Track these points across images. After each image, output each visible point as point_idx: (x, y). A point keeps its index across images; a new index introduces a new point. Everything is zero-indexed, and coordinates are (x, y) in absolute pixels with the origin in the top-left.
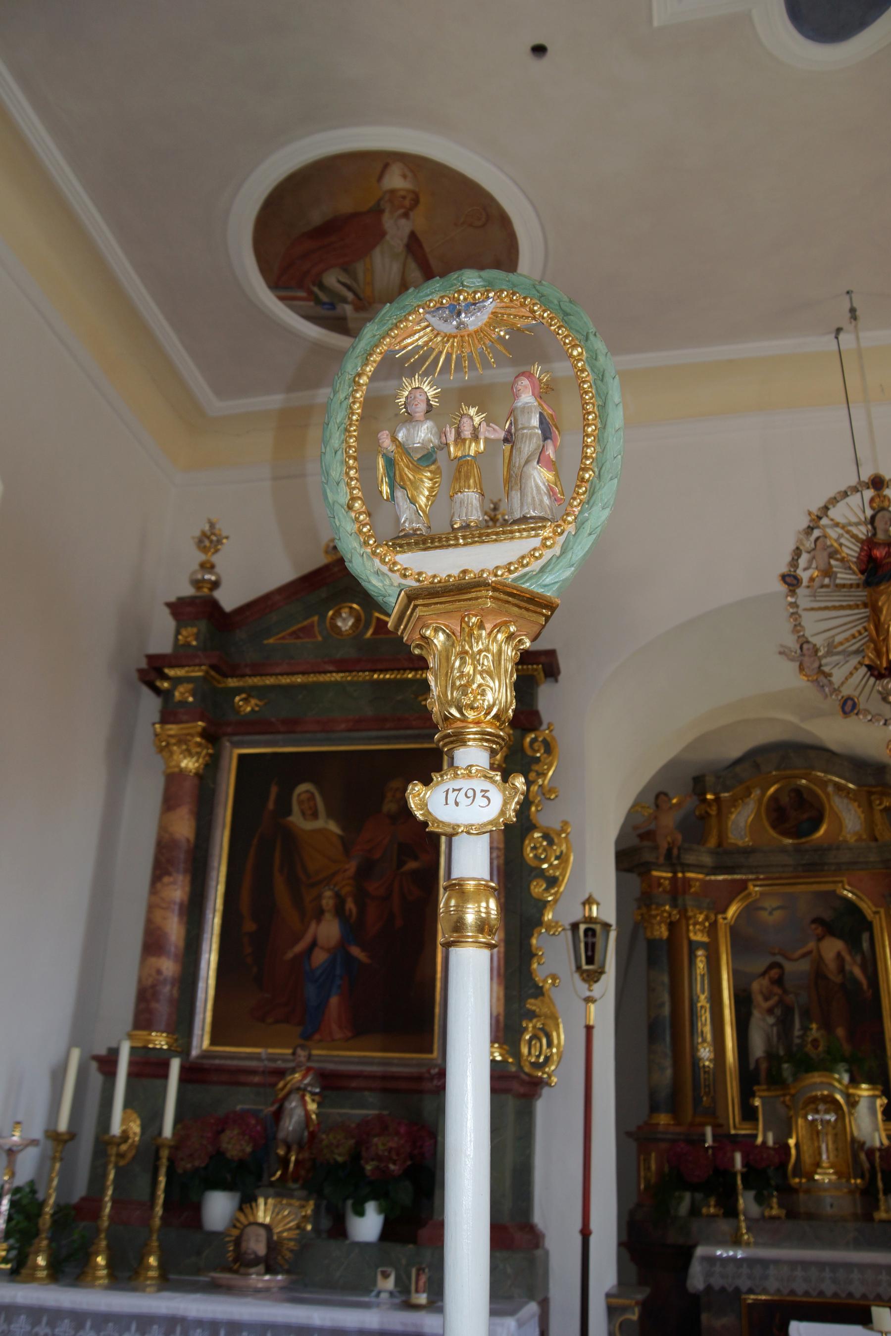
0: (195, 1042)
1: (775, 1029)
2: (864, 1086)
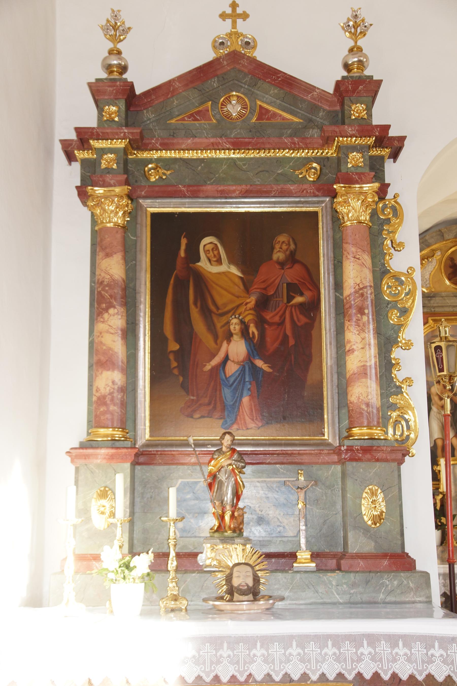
0: (139, 432)
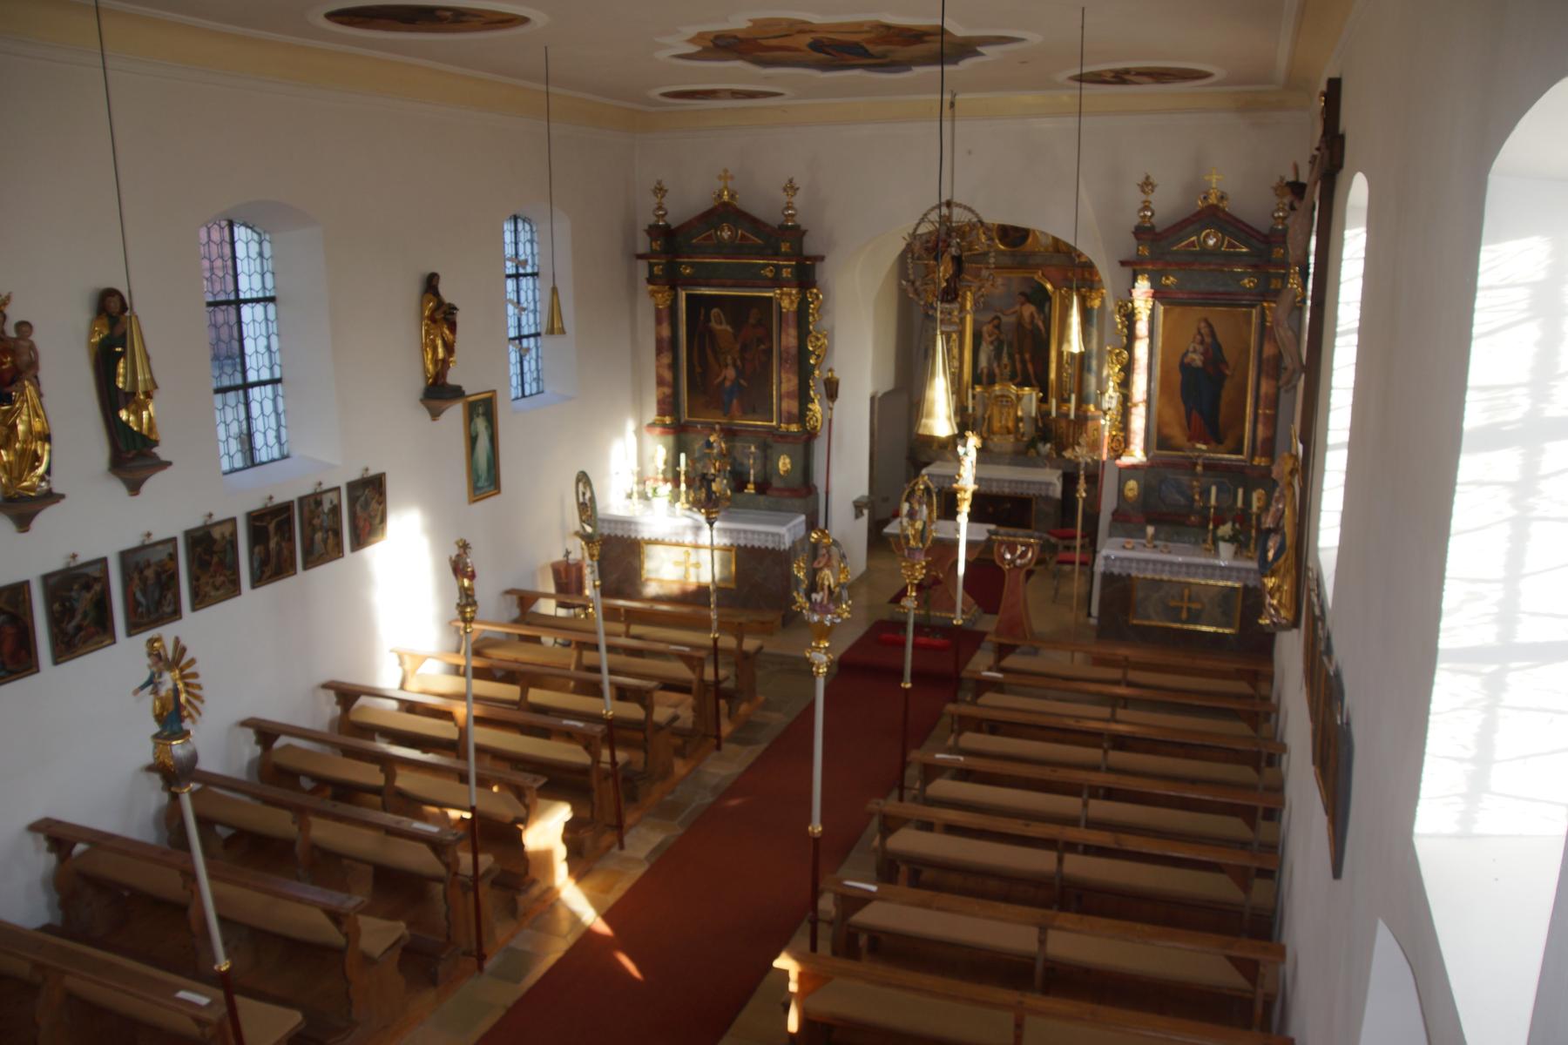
1: (993, 353)
2: (1027, 389)
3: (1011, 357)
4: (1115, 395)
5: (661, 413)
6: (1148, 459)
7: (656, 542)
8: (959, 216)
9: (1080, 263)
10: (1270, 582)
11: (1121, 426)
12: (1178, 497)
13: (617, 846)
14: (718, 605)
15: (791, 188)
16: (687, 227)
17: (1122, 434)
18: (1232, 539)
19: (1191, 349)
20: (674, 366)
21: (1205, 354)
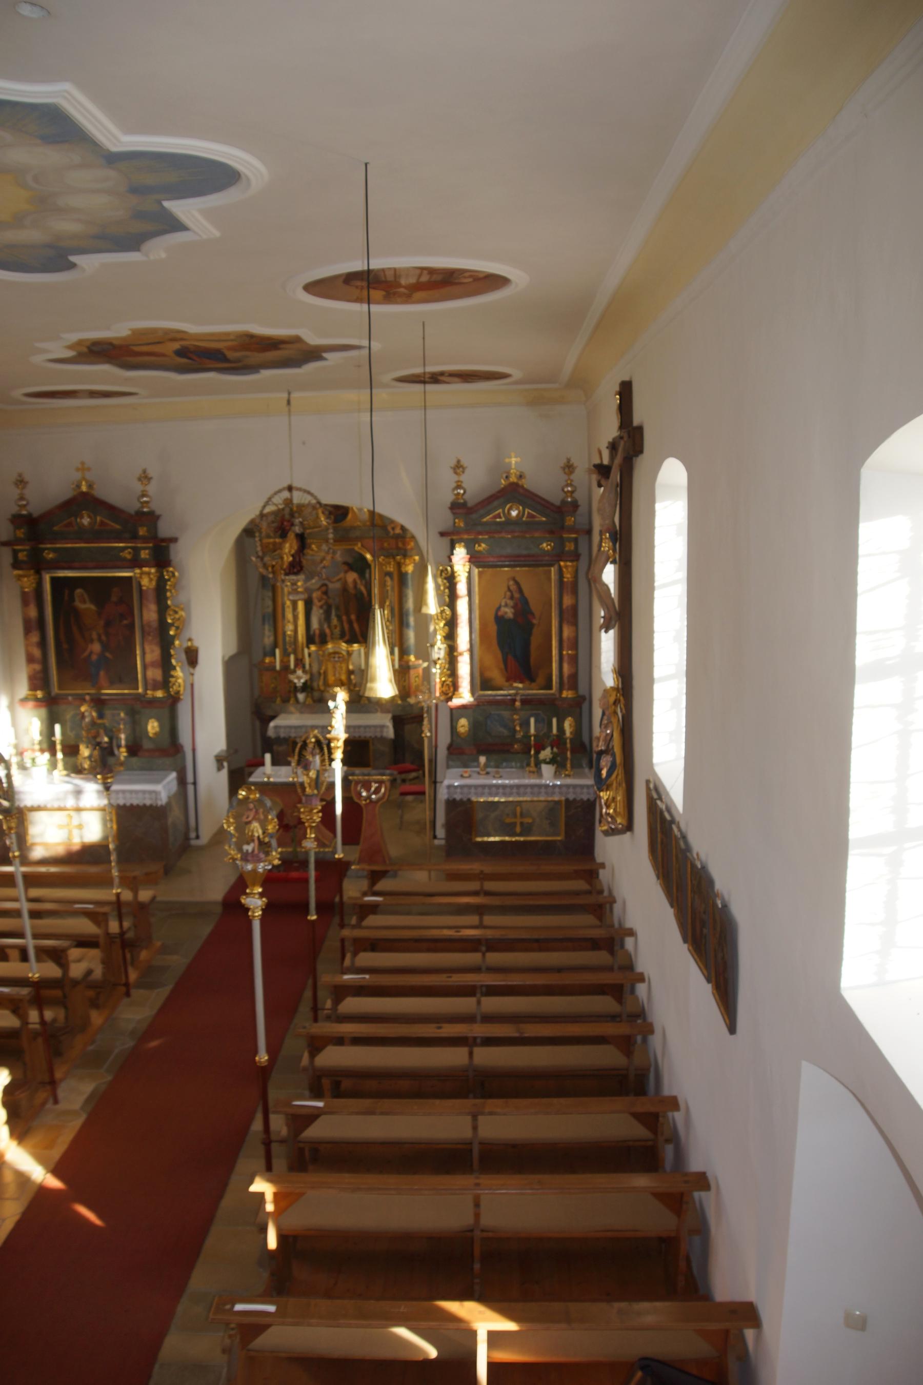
2: (355, 645)
3: (339, 617)
4: (443, 646)
5: (33, 687)
6: (475, 699)
7: (38, 809)
8: (298, 498)
9: (394, 534)
10: (604, 795)
11: (449, 672)
12: (502, 729)
13: (51, 1101)
14: (119, 862)
15: (145, 478)
16: (48, 516)
17: (450, 679)
18: (552, 761)
19: (503, 604)
20: (43, 644)
21: (514, 607)
